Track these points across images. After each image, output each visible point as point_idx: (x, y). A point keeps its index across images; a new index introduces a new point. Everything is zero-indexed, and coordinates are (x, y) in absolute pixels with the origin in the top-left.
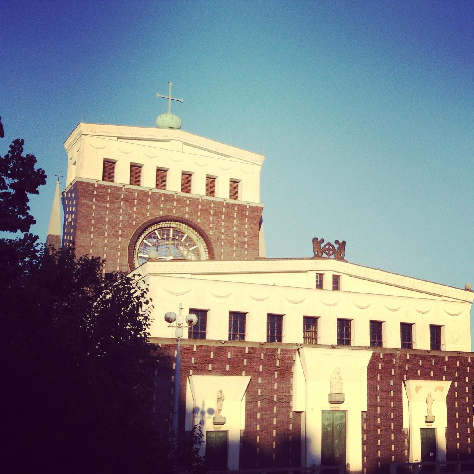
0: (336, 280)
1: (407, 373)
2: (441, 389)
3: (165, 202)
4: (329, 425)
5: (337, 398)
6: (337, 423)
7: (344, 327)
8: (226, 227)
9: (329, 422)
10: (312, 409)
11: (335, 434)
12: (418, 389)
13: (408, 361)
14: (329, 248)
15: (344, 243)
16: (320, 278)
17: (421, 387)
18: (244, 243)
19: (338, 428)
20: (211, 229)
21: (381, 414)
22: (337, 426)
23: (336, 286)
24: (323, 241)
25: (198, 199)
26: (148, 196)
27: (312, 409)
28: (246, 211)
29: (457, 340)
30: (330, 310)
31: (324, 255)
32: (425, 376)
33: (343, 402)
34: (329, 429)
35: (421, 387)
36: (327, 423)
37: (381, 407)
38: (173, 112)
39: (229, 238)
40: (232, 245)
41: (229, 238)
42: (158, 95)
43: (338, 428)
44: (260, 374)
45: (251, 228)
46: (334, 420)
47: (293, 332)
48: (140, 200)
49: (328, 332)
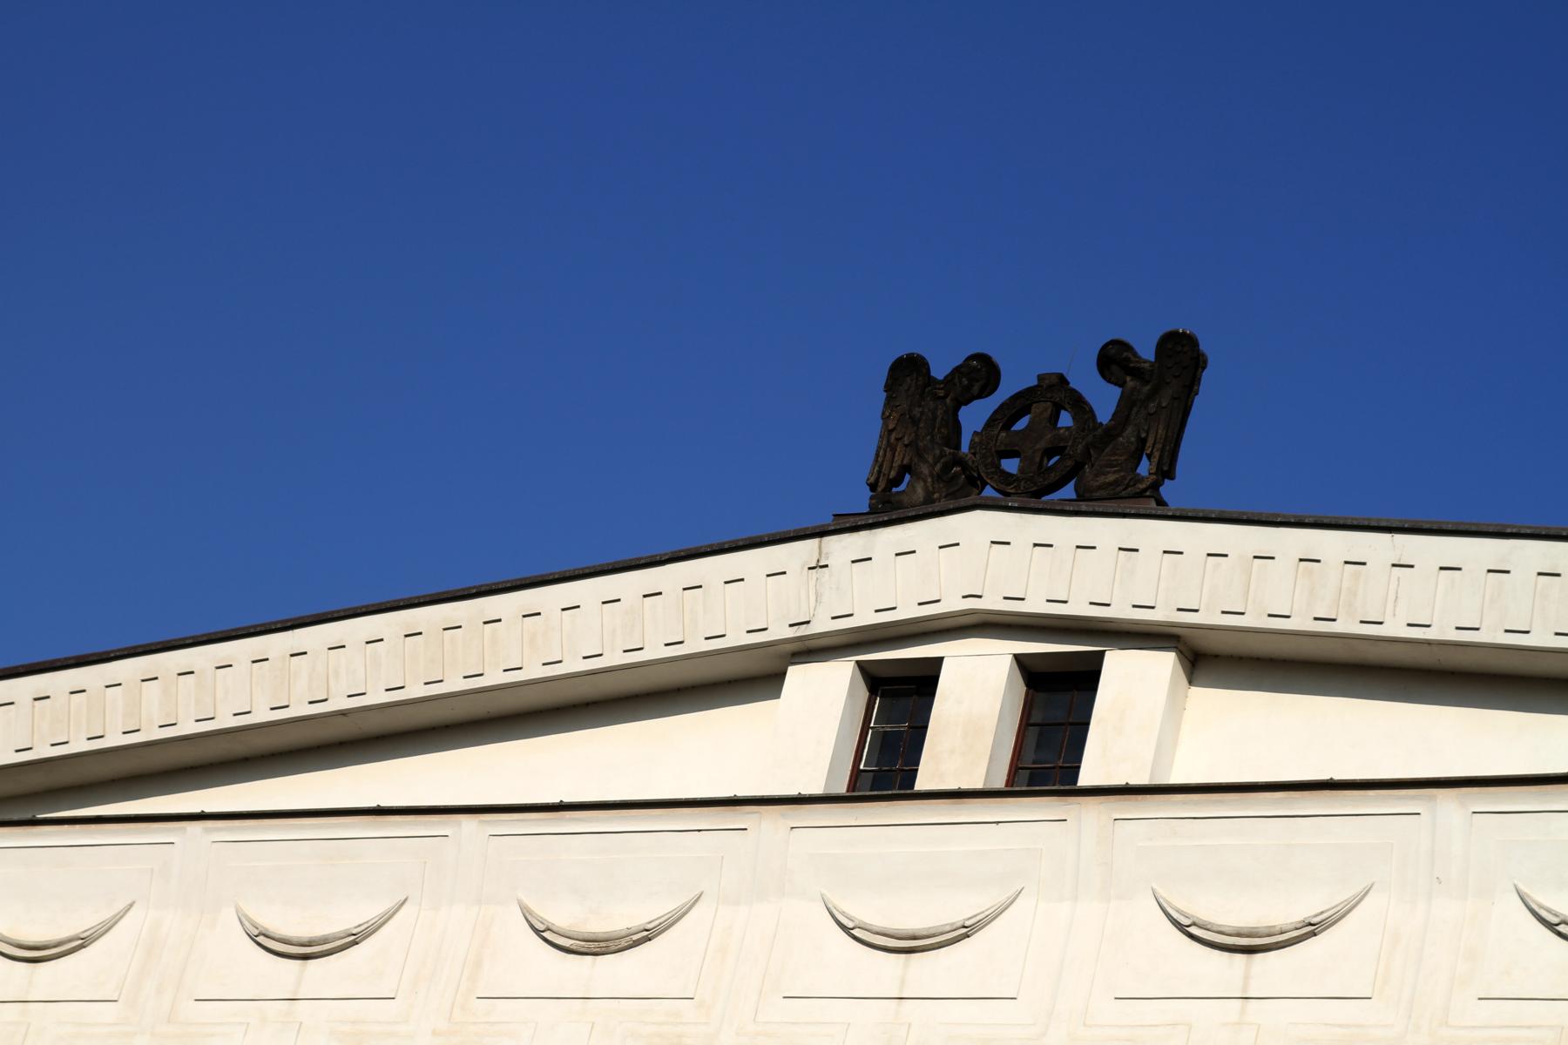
0: (1057, 698)
15: (1182, 357)
23: (1048, 749)
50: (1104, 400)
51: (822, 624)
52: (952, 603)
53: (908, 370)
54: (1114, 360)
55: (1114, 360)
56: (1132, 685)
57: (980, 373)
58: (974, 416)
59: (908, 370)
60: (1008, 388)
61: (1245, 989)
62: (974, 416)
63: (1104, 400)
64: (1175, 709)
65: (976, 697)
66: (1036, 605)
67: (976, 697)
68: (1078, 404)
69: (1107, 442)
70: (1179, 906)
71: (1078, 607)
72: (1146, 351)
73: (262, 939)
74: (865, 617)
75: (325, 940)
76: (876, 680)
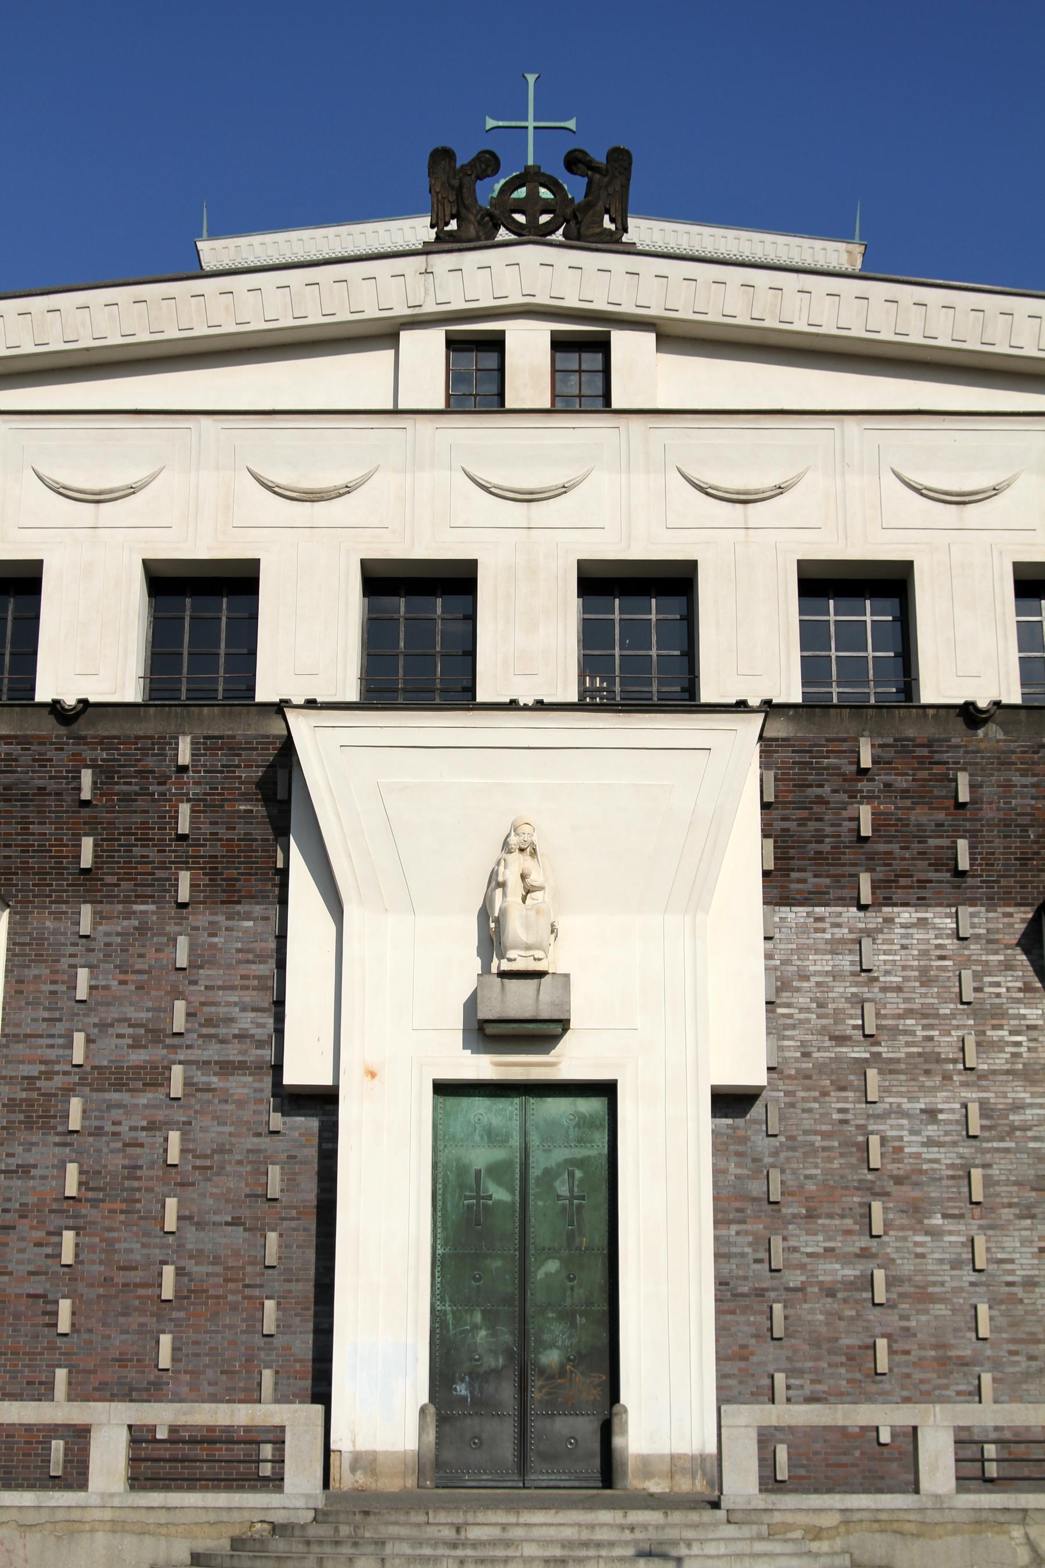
4: (496, 1171)
5: (519, 1001)
6: (560, 1155)
9: (499, 1154)
10: (373, 1075)
11: (541, 1232)
14: (533, 194)
16: (476, 356)
19: (563, 1190)
22: (550, 1175)
24: (487, 163)
27: (373, 1075)
30: (528, 514)
33: (564, 1024)
34: (500, 1194)
36: (481, 1157)
42: (491, 123)
43: (563, 1190)
44: (87, 883)
46: (534, 1139)
47: (307, 643)
49: (526, 636)
51: (430, 307)
52: (516, 299)
54: (575, 162)
56: (629, 349)
57: (487, 163)
59: (442, 156)
61: (746, 522)
66: (572, 302)
68: (553, 185)
69: (589, 206)
70: (55, 478)
71: (600, 305)
72: (599, 156)
73: (62, 491)
74: (458, 304)
75: (111, 491)
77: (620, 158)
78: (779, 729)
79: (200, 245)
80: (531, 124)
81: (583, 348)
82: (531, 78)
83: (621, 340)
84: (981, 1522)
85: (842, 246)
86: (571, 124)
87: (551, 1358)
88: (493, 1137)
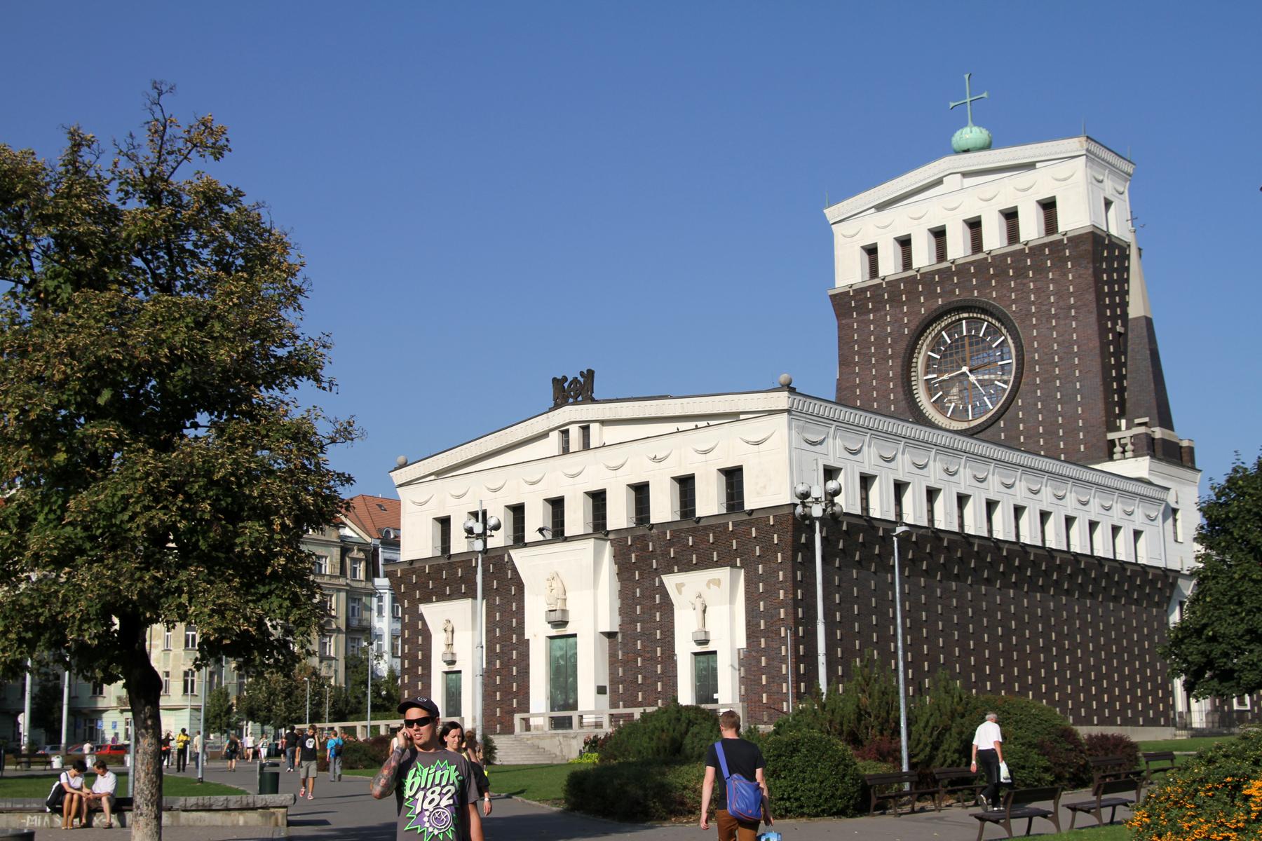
1: (676, 561)
2: (718, 582)
3: (940, 283)
4: (561, 657)
7: (598, 499)
8: (1037, 291)
12: (679, 587)
13: (671, 543)
17: (682, 585)
18: (1070, 307)
20: (1014, 301)
21: (643, 634)
25: (986, 259)
26: (918, 282)
28: (1064, 250)
29: (765, 487)
31: (571, 400)
32: (705, 563)
35: (682, 585)
36: (558, 653)
37: (642, 622)
38: (976, 124)
39: (1044, 308)
40: (1050, 317)
41: (1044, 308)
42: (952, 105)
45: (1080, 276)
48: (908, 293)
50: (582, 380)
53: (554, 380)
54: (582, 374)
55: (582, 374)
56: (594, 428)
57: (565, 379)
58: (566, 385)
59: (554, 380)
60: (570, 379)
62: (566, 385)
63: (582, 380)
64: (601, 430)
65: (575, 432)
67: (575, 432)
76: (563, 432)
77: (591, 374)
78: (611, 536)
79: (826, 211)
80: (968, 100)
81: (585, 429)
82: (967, 76)
83: (592, 426)
84: (553, 736)
85: (1076, 140)
86: (985, 95)
87: (571, 701)
88: (561, 649)
